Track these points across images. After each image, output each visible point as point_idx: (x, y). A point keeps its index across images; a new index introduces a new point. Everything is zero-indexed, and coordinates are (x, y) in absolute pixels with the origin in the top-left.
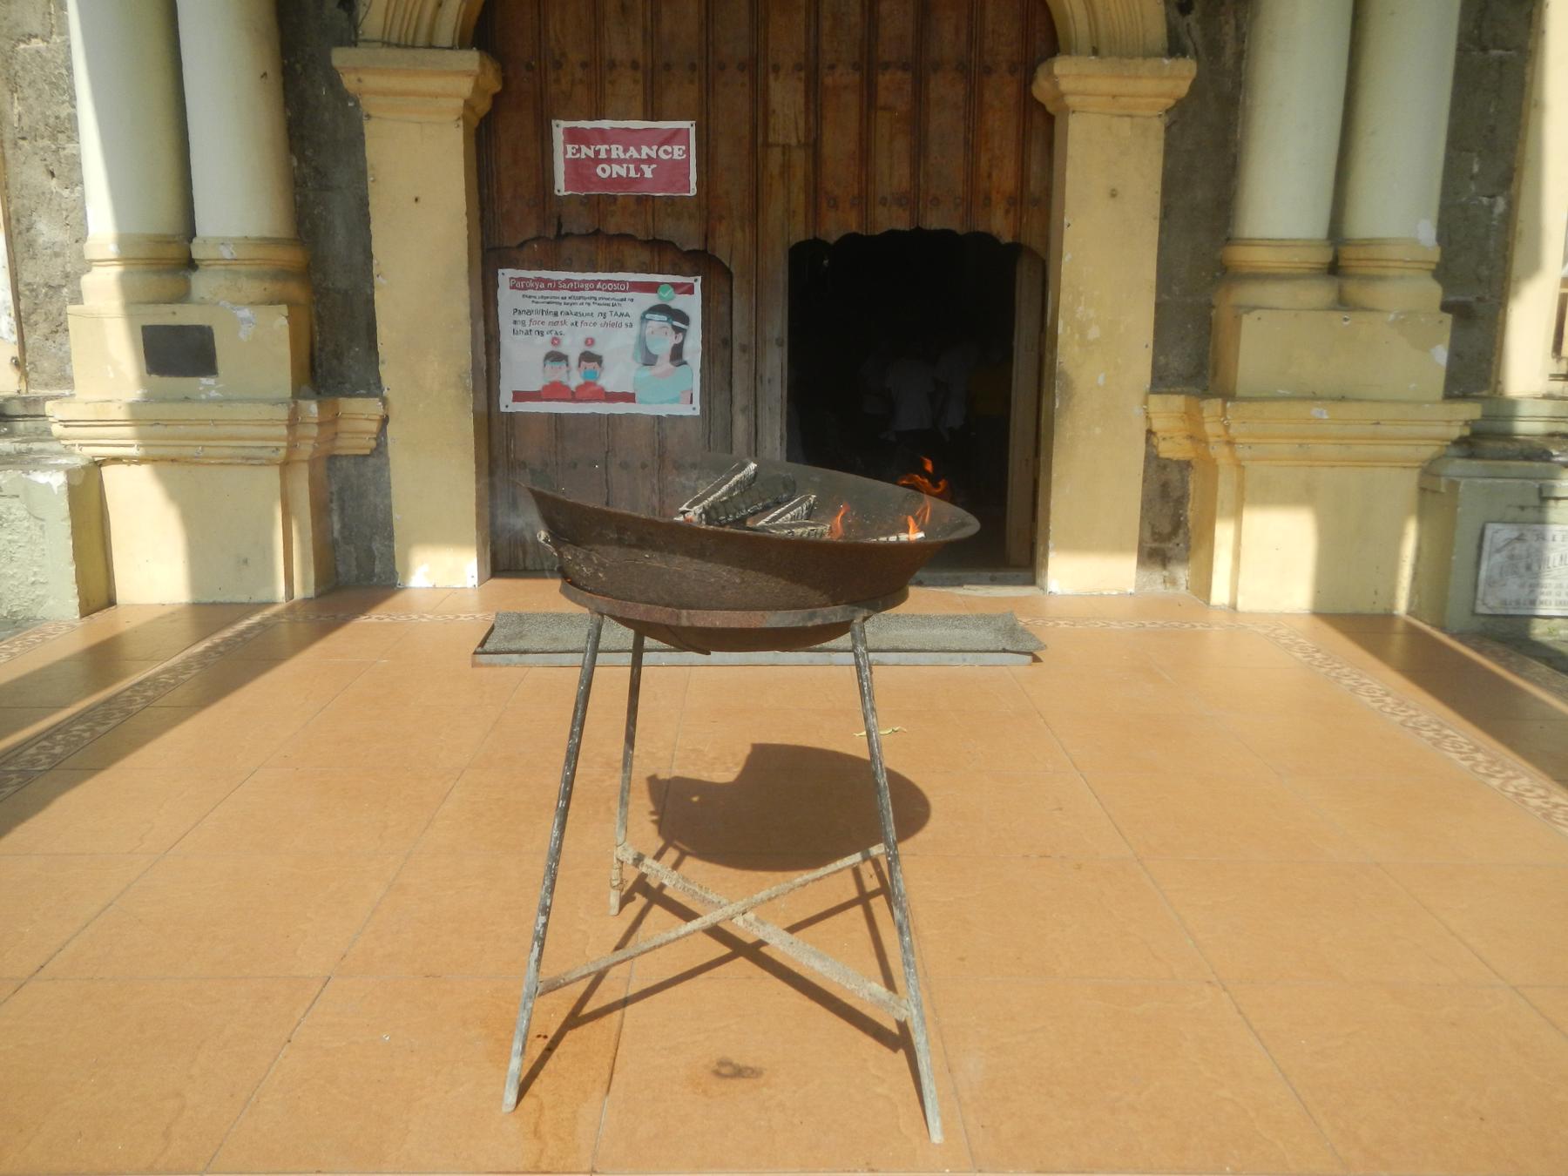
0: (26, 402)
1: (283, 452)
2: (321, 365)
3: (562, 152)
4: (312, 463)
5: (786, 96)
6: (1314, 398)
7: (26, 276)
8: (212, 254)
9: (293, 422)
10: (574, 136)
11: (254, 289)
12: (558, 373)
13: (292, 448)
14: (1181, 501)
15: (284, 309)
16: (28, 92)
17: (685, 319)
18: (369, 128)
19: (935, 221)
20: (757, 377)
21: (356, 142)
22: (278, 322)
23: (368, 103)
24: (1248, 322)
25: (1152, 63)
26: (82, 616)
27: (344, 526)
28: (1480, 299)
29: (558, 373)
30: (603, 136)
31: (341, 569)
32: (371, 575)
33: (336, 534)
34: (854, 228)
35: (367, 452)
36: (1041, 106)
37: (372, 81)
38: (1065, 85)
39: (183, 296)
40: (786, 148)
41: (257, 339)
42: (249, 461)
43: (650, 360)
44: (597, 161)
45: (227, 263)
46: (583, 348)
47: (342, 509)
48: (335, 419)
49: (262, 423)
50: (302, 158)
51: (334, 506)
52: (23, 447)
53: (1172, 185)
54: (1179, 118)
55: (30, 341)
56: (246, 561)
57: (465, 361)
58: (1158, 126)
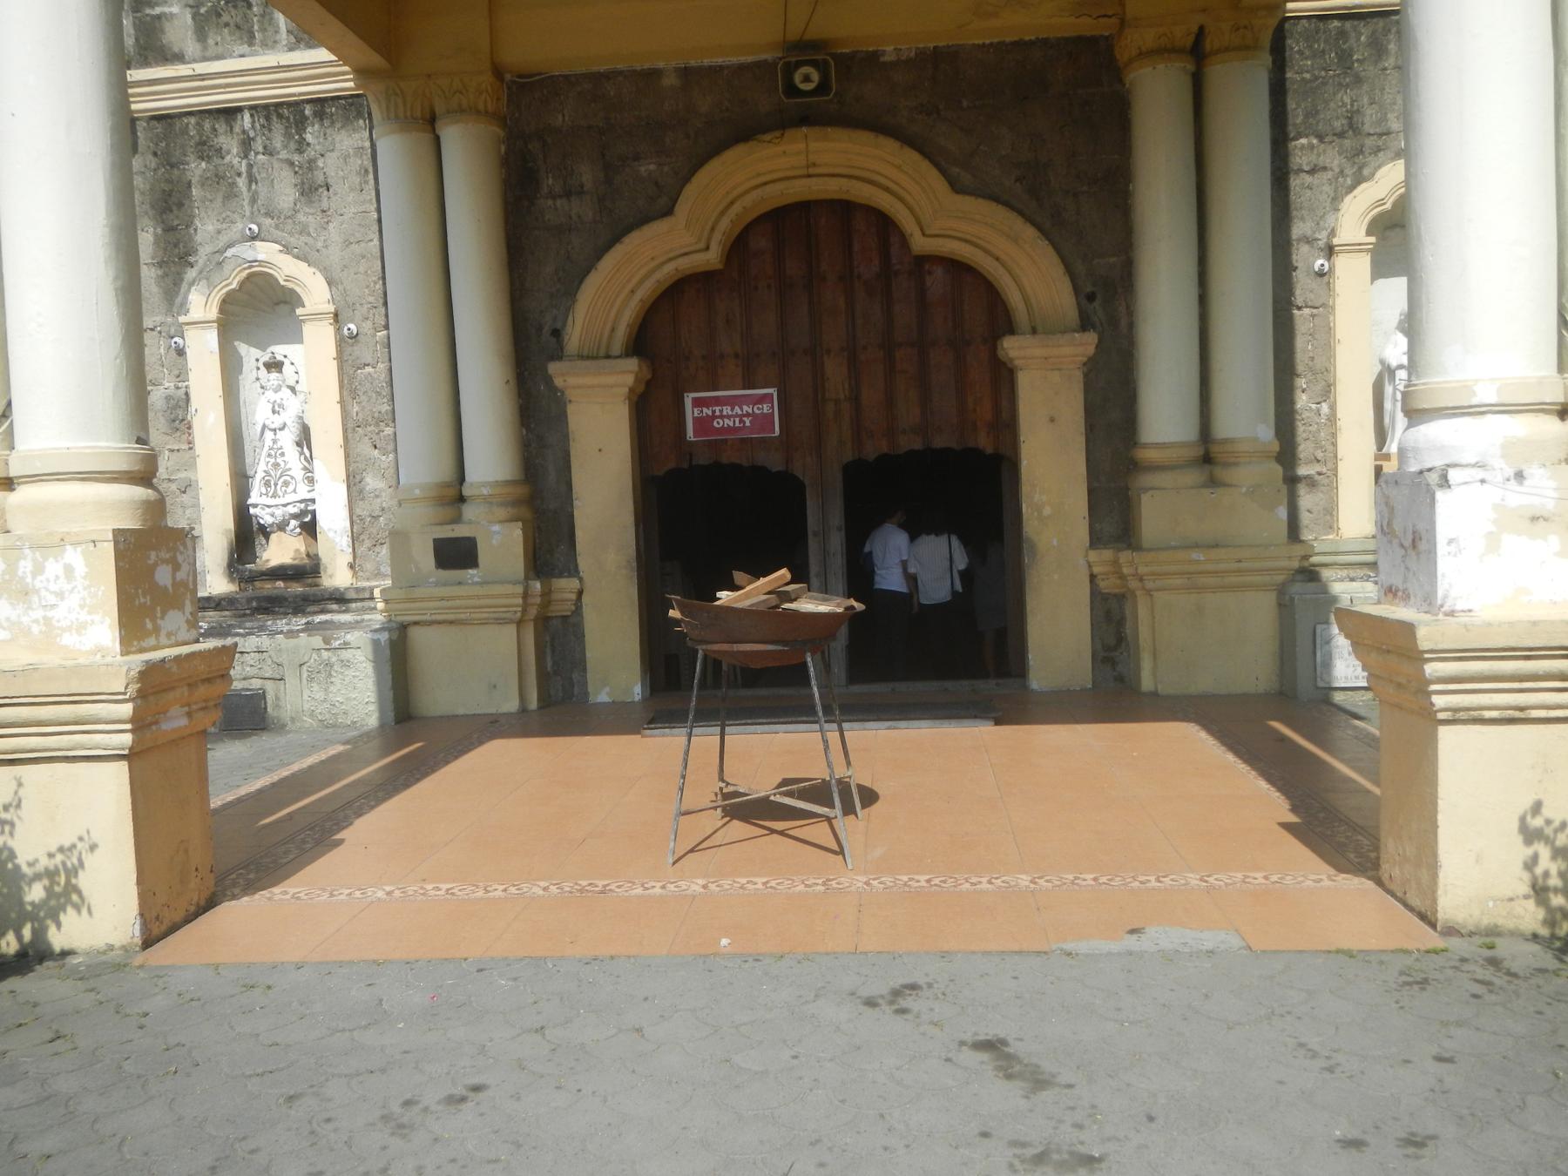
0: (358, 590)
3: (691, 412)
4: (536, 620)
5: (835, 371)
6: (1196, 546)
7: (358, 511)
8: (476, 492)
9: (525, 595)
10: (698, 403)
11: (502, 513)
13: (524, 611)
14: (1121, 622)
15: (520, 524)
16: (363, 398)
18: (570, 409)
19: (939, 442)
22: (517, 532)
23: (570, 394)
24: (1145, 498)
25: (1067, 336)
28: (1320, 474)
30: (717, 401)
34: (885, 450)
36: (1004, 364)
37: (572, 381)
38: (1012, 354)
39: (457, 519)
40: (837, 402)
41: (502, 542)
42: (500, 622)
44: (714, 417)
45: (487, 500)
47: (553, 652)
49: (507, 596)
50: (528, 429)
51: (548, 651)
53: (1091, 413)
54: (1092, 370)
55: (359, 552)
58: (1079, 375)
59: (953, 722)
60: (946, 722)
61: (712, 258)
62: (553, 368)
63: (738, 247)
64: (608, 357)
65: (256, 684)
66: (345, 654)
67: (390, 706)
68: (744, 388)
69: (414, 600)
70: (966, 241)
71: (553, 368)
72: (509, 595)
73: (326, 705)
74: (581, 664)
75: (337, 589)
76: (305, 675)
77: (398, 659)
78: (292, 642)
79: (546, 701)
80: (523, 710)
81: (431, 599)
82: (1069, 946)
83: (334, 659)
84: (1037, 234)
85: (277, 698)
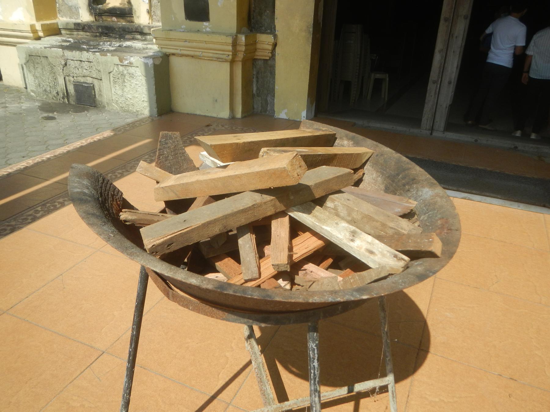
1: (230, 57)
2: (253, 18)
9: (235, 44)
13: (235, 54)
20: (450, 35)
26: (158, 116)
27: (258, 89)
31: (255, 106)
32: (266, 111)
33: (254, 92)
35: (268, 58)
42: (219, 60)
47: (257, 81)
48: (255, 43)
49: (222, 44)
51: (255, 80)
52: (145, 46)
56: (216, 101)
59: (522, 205)
60: (516, 204)
65: (89, 80)
66: (132, 70)
67: (155, 105)
69: (170, 40)
72: (224, 44)
73: (123, 99)
74: (271, 91)
75: (139, 26)
76: (112, 79)
77: (161, 75)
78: (103, 58)
80: (233, 118)
81: (179, 40)
83: (125, 72)
85: (100, 91)
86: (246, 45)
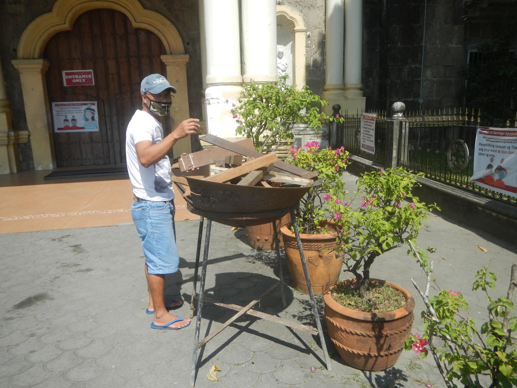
3: (65, 77)
5: (111, 64)
9: (8, 136)
10: (67, 74)
12: (67, 124)
13: (9, 140)
17: (93, 110)
20: (112, 122)
21: (18, 79)
23: (20, 70)
29: (67, 124)
37: (21, 66)
43: (87, 120)
46: (72, 118)
48: (18, 135)
57: (46, 122)
61: (66, 26)
62: (14, 62)
63: (77, 22)
64: (33, 58)
68: (82, 69)
70: (149, 25)
71: (14, 62)
74: (32, 158)
79: (20, 170)
80: (12, 173)
82: (117, 224)
84: (170, 23)
86: (14, 137)
